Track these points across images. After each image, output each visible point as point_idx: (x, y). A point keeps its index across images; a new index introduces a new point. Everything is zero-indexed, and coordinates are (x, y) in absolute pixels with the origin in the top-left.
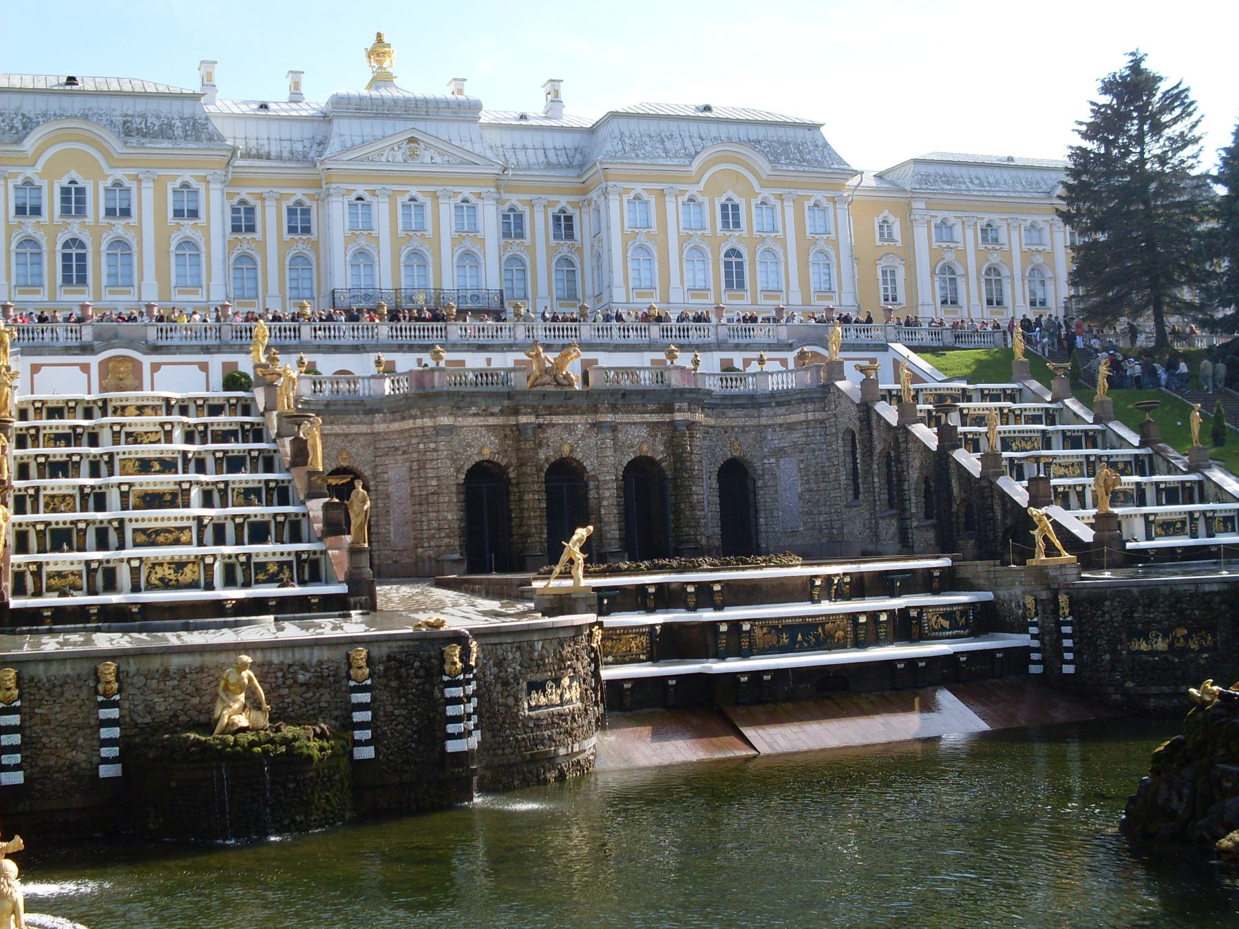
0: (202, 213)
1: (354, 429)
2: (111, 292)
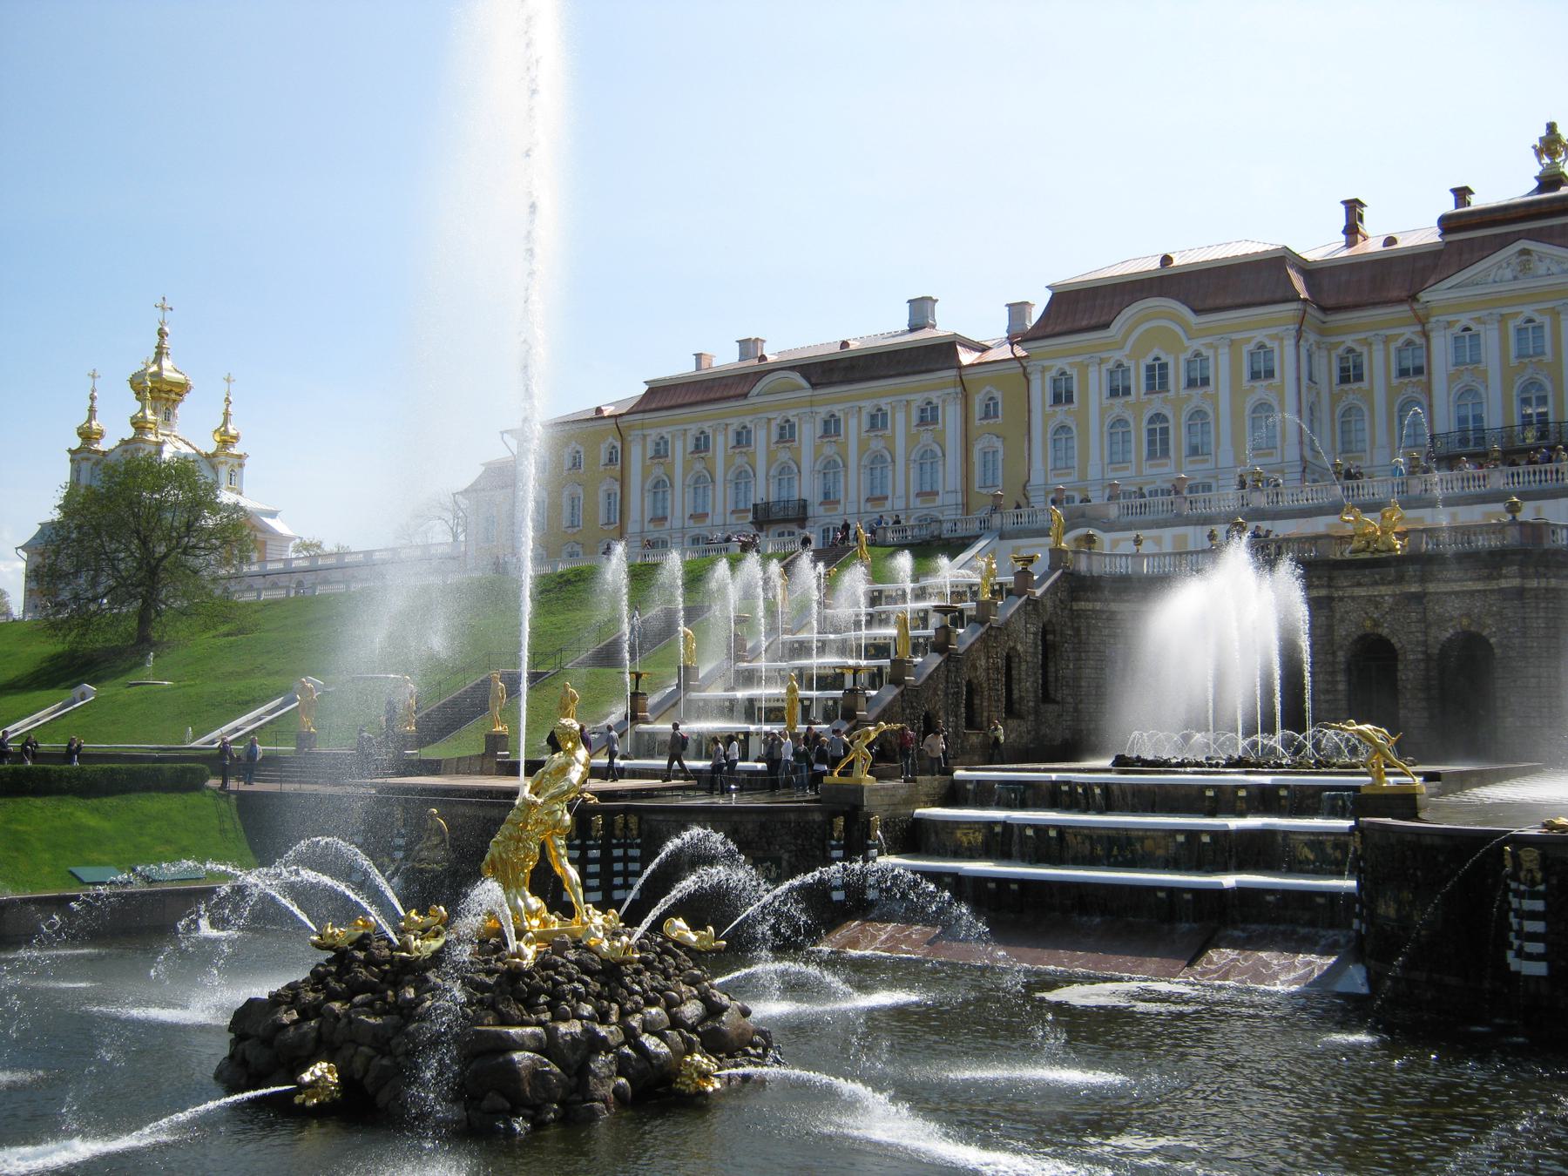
0: (1277, 373)
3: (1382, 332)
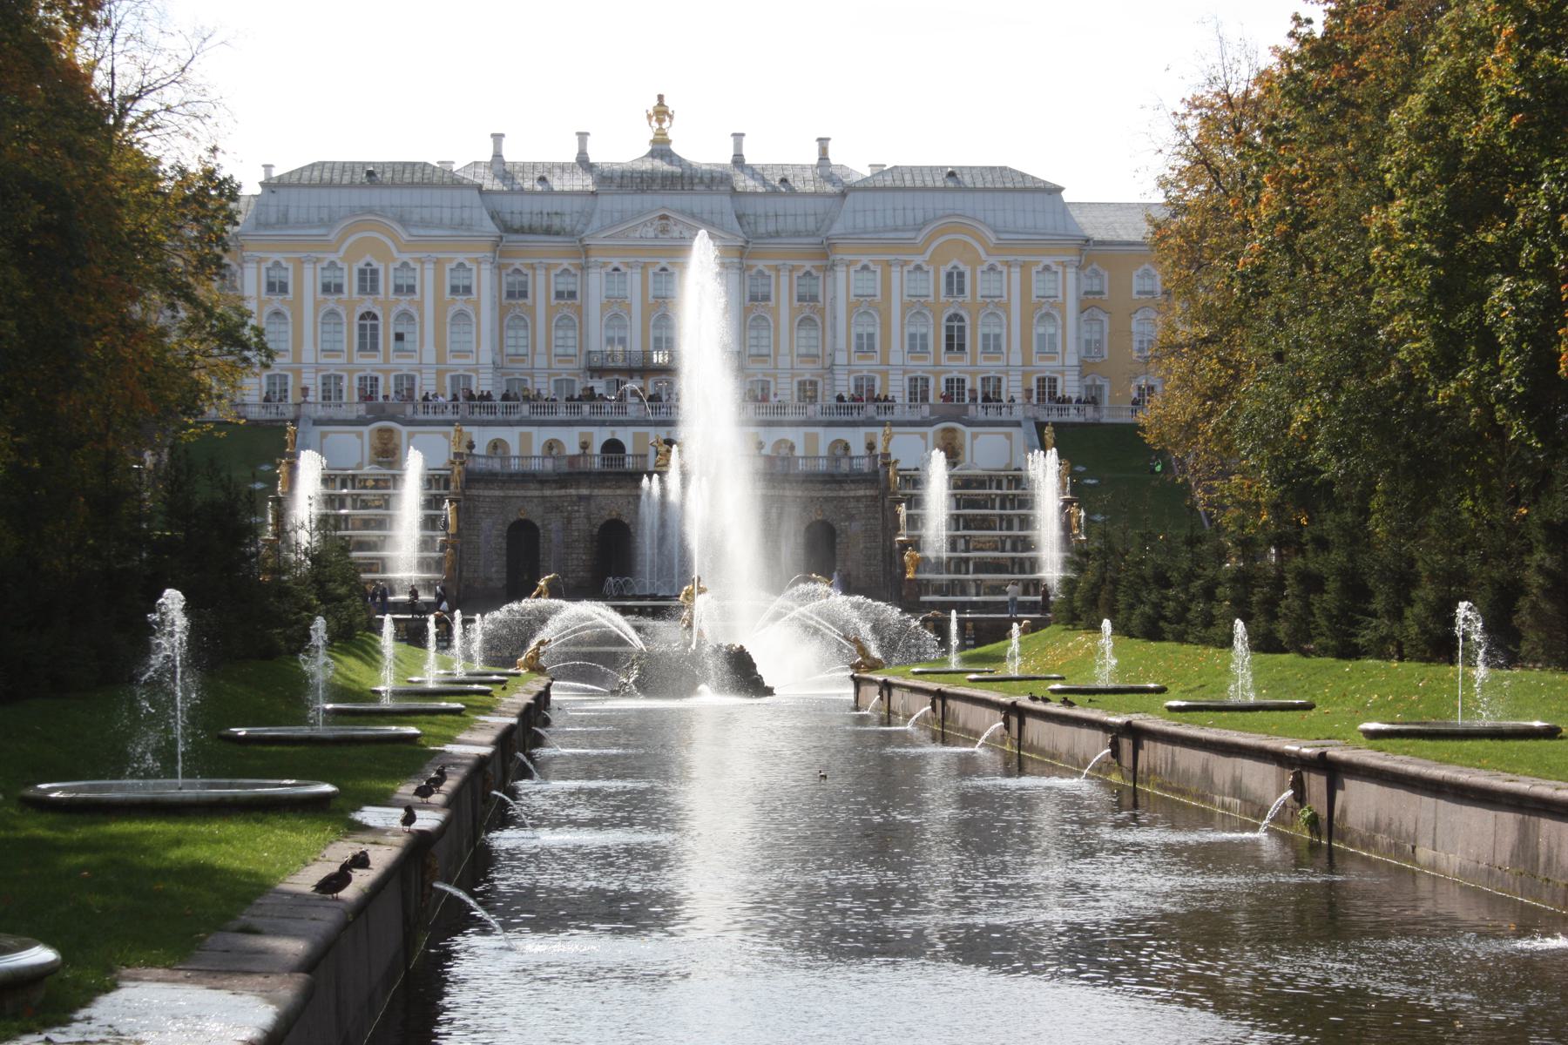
1: (530, 493)
2: (398, 357)
3: (544, 261)
